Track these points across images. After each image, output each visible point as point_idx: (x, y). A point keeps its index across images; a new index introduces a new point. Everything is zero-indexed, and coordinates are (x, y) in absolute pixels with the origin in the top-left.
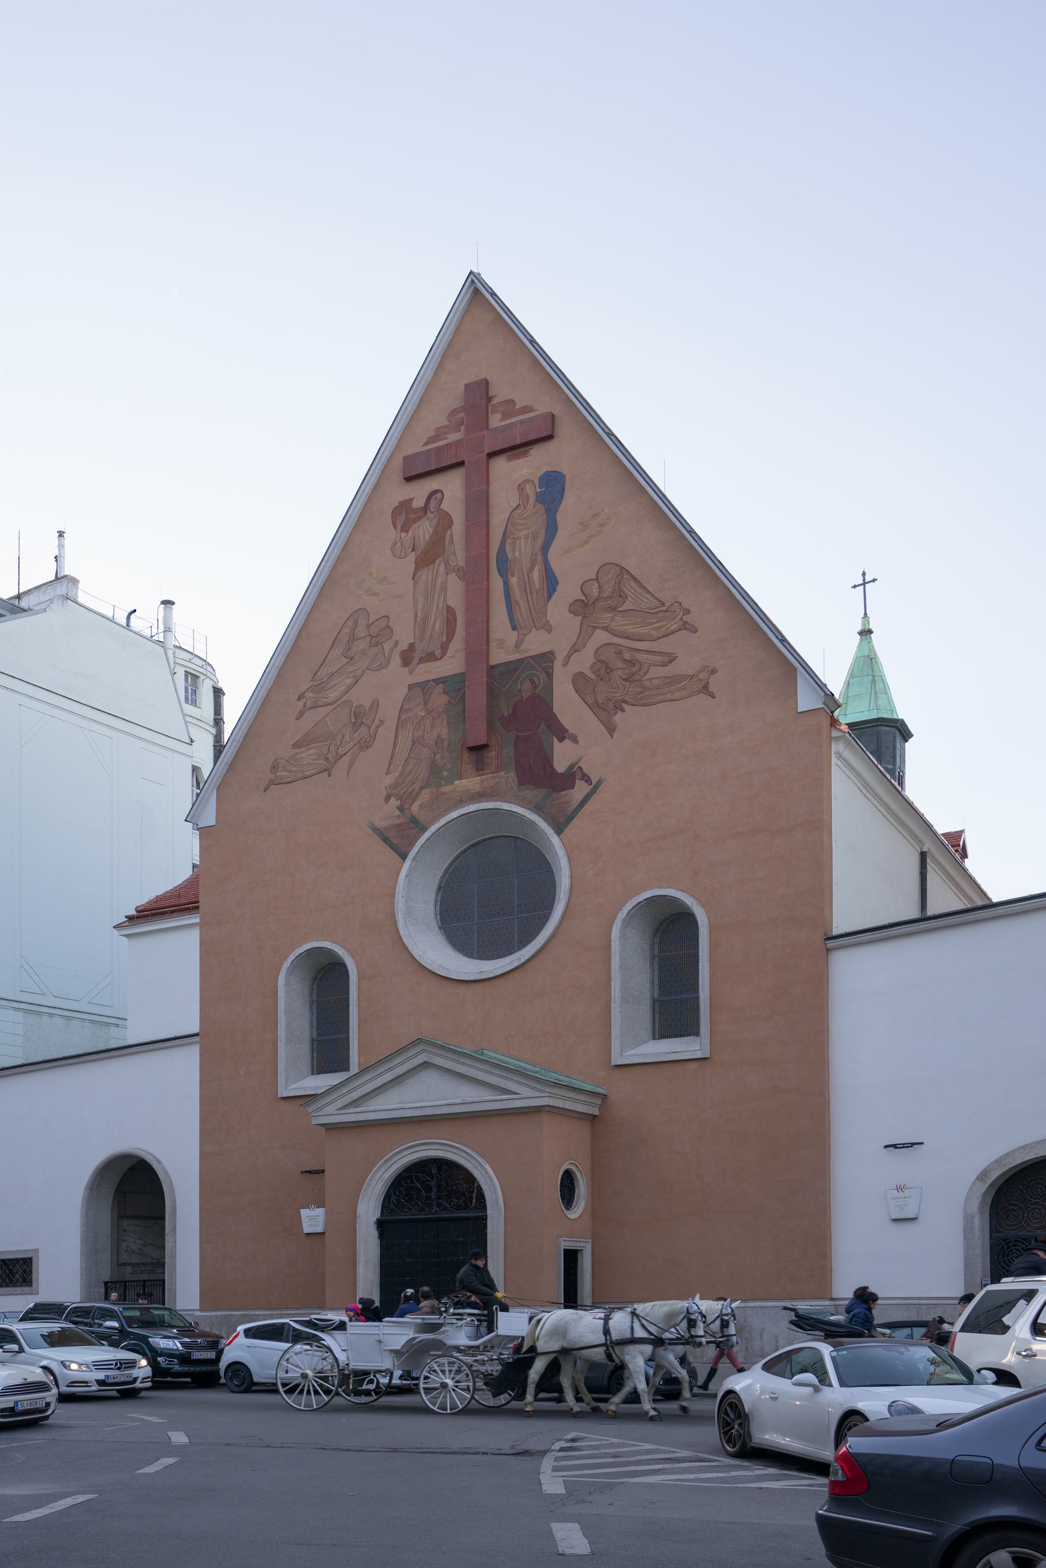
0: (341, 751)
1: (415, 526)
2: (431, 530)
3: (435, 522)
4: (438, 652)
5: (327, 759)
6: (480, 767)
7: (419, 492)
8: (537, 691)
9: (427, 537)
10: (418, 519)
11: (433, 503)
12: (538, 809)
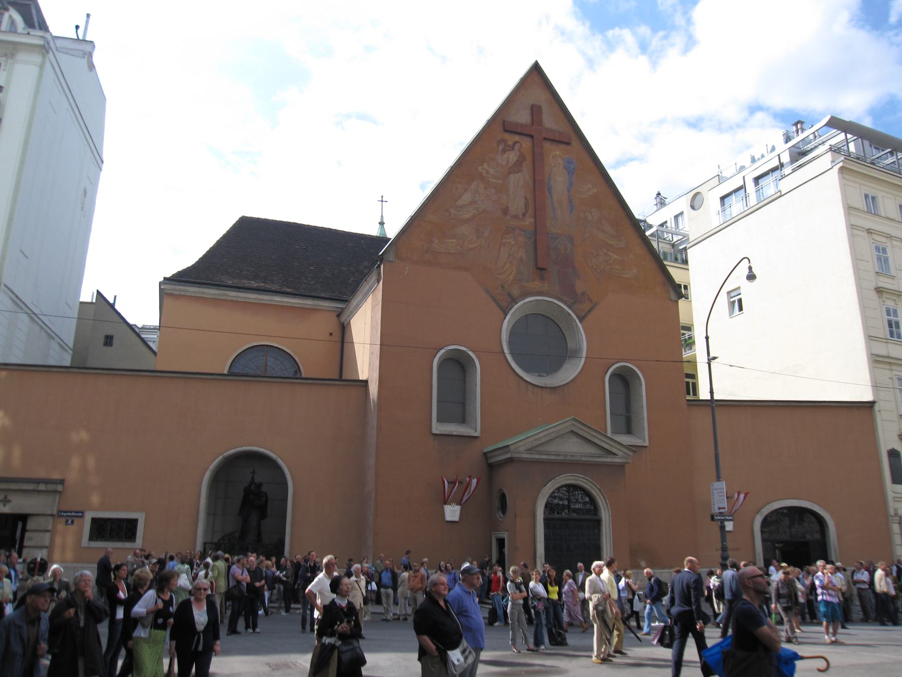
0: (470, 246)
1: (508, 153)
2: (516, 158)
3: (518, 154)
4: (521, 216)
5: (462, 247)
6: (542, 279)
7: (511, 139)
8: (568, 252)
9: (515, 161)
10: (509, 150)
11: (517, 147)
12: (569, 307)
